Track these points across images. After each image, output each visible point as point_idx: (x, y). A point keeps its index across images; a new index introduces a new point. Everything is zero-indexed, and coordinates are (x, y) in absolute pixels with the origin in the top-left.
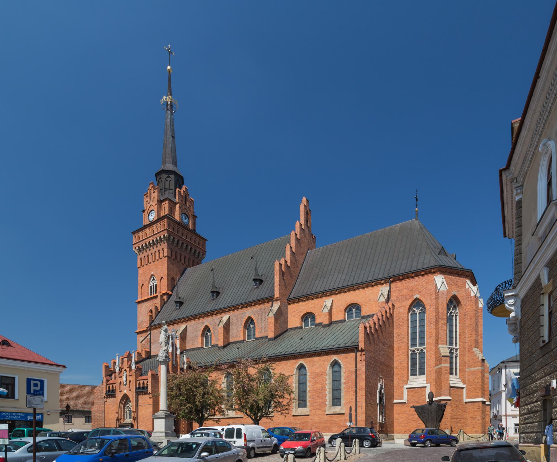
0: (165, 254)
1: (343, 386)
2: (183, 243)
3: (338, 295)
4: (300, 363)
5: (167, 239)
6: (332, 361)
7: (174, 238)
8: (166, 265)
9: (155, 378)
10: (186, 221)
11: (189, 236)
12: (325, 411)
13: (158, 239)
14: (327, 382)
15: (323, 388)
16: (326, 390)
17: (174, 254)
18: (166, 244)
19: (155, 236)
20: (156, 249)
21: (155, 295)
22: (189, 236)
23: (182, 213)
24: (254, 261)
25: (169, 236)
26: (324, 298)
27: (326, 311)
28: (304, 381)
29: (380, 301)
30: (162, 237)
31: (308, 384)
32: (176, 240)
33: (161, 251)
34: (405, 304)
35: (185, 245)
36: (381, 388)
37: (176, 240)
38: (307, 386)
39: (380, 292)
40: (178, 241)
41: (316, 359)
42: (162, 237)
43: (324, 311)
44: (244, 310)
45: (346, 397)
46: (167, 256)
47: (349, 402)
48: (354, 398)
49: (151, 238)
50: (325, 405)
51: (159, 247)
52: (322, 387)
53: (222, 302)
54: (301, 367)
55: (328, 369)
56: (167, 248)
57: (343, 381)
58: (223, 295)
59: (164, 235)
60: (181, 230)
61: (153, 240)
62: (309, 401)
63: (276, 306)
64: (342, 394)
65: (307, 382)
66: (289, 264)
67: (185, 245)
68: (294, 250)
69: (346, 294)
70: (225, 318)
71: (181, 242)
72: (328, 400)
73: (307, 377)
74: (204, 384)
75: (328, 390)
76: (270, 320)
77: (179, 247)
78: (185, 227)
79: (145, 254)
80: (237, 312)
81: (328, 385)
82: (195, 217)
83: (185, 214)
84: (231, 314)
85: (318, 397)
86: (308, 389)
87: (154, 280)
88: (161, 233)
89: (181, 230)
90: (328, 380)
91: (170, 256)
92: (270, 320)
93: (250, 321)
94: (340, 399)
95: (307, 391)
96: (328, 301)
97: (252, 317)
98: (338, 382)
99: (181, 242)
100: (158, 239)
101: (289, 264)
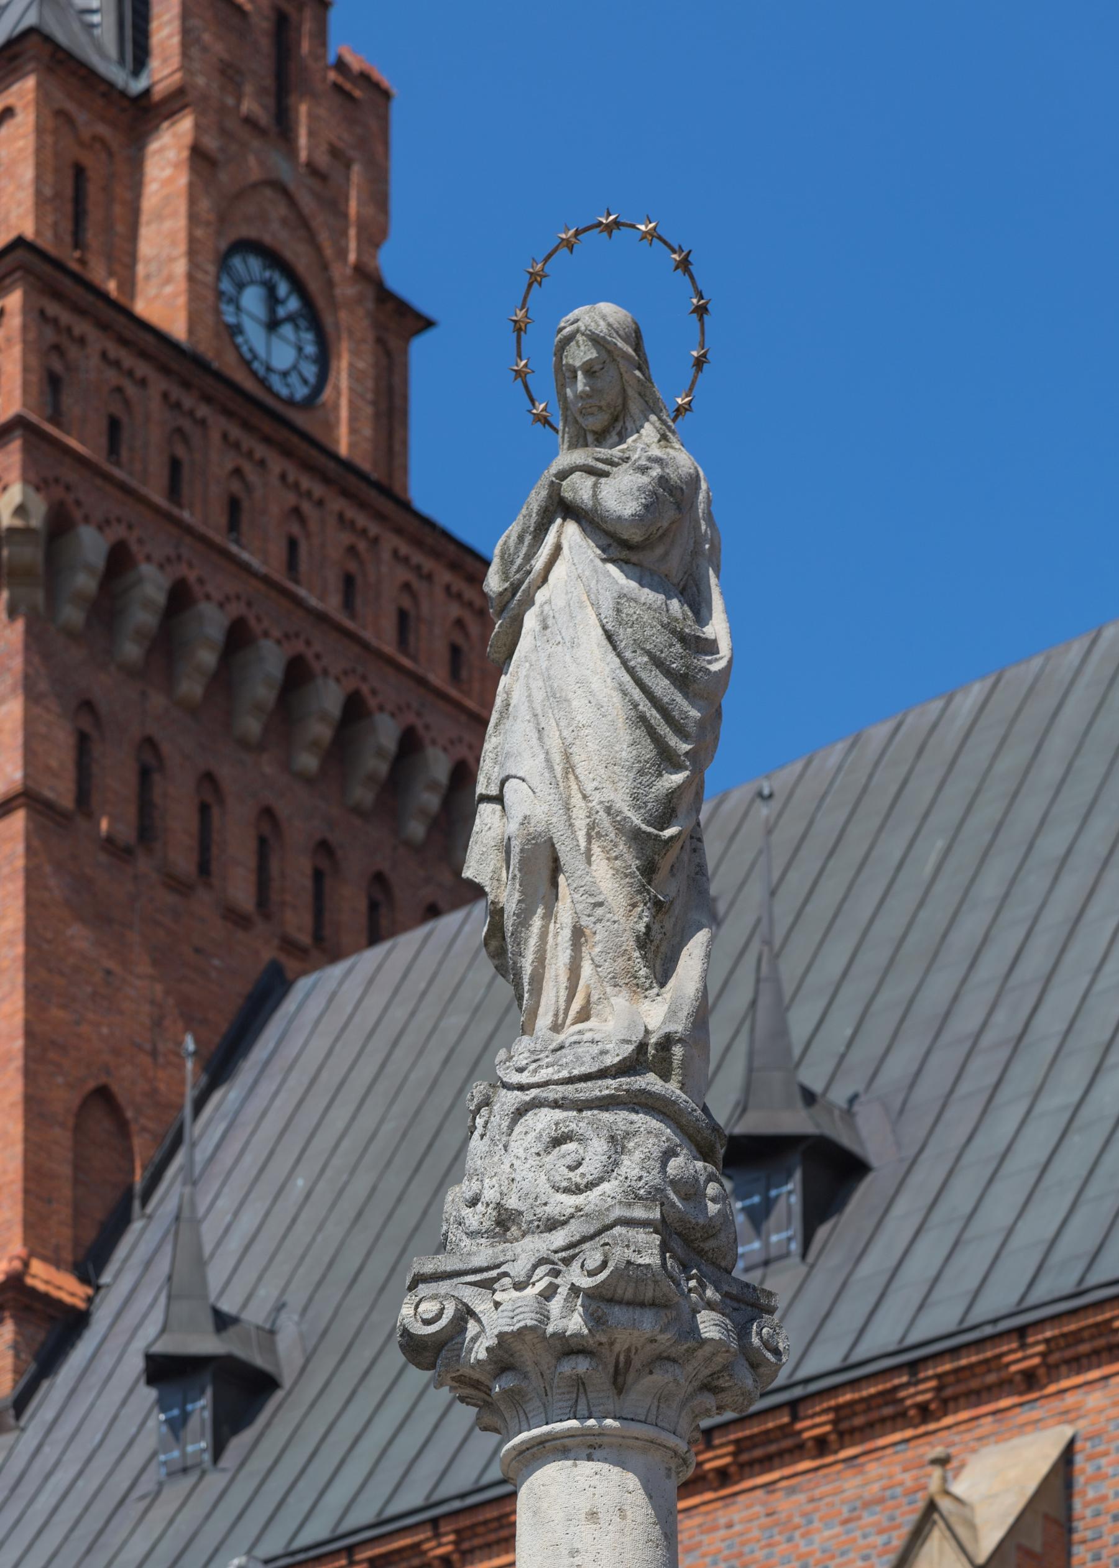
2: (238, 638)
7: (119, 560)
10: (282, 354)
11: (327, 542)
22: (327, 542)
23: (229, 247)
32: (152, 584)
35: (269, 661)
37: (152, 584)
40: (180, 598)
60: (220, 462)
67: (269, 661)
71: (211, 622)
78: (279, 425)
82: (399, 321)
83: (273, 258)
89: (220, 462)
91: (62, 792)
99: (211, 622)
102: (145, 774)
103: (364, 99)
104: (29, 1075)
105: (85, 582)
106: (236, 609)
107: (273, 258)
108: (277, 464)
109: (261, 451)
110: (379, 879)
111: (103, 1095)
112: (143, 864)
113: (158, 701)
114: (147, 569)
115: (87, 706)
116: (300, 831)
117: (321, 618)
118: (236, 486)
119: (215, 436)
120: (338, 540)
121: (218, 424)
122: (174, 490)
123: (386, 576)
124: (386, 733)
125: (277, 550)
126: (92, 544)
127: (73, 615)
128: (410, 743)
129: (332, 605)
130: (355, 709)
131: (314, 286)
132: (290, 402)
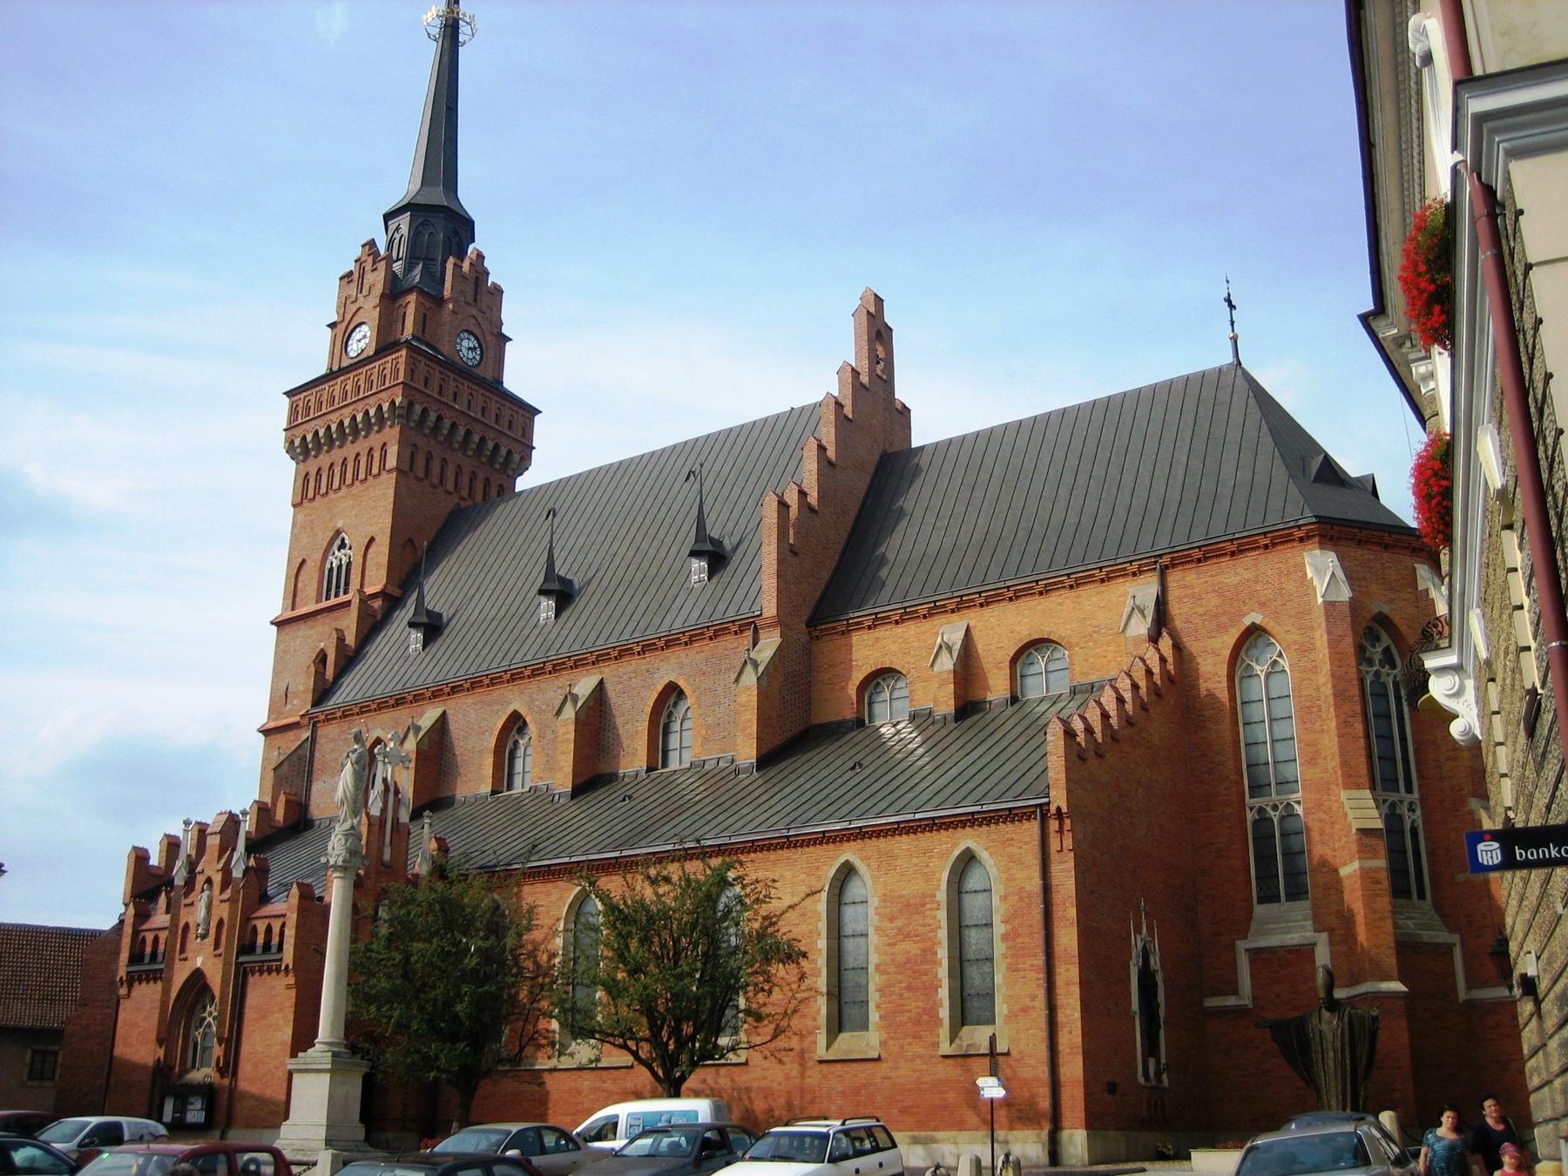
0: (392, 462)
1: (999, 949)
3: (987, 611)
4: (842, 860)
5: (402, 414)
6: (956, 853)
7: (425, 411)
8: (391, 499)
9: (313, 909)
12: (936, 1045)
13: (372, 412)
14: (943, 934)
15: (928, 954)
16: (936, 963)
18: (397, 429)
19: (360, 405)
20: (362, 446)
25: (411, 404)
26: (938, 620)
27: (947, 663)
28: (860, 928)
29: (1131, 632)
30: (385, 407)
31: (873, 938)
32: (433, 416)
33: (377, 455)
34: (1215, 643)
36: (1146, 953)
37: (433, 416)
38: (871, 949)
39: (1130, 602)
40: (440, 418)
41: (903, 843)
42: (385, 407)
43: (936, 668)
44: (651, 659)
45: (1013, 989)
47: (1025, 1010)
48: (1041, 994)
49: (347, 412)
50: (939, 1022)
51: (375, 440)
52: (924, 950)
53: (584, 627)
54: (847, 871)
55: (944, 886)
56: (400, 443)
57: (999, 928)
58: (584, 600)
59: (393, 402)
61: (354, 418)
62: (878, 1006)
64: (998, 979)
65: (871, 931)
66: (813, 498)
68: (831, 453)
69: (1011, 606)
70: (584, 686)
72: (946, 1003)
73: (871, 911)
74: (497, 925)
75: (945, 963)
76: (743, 699)
77: (441, 438)
79: (324, 460)
80: (630, 666)
81: (945, 943)
84: (608, 671)
85: (909, 988)
86: (874, 959)
88: (383, 395)
90: (944, 924)
91: (406, 467)
92: (743, 699)
93: (673, 692)
94: (990, 995)
95: (871, 968)
96: (951, 630)
97: (682, 683)
98: (985, 932)
100: (372, 412)
101: (813, 498)
105: (416, 417)
107: (471, 333)
110: (487, 479)
111: (410, 540)
115: (415, 445)
116: (467, 469)
117: (475, 419)
120: (481, 399)
122: (440, 393)
123: (493, 407)
124: (490, 445)
125: (466, 403)
126: (418, 409)
128: (496, 447)
129: (479, 416)
130: (483, 440)
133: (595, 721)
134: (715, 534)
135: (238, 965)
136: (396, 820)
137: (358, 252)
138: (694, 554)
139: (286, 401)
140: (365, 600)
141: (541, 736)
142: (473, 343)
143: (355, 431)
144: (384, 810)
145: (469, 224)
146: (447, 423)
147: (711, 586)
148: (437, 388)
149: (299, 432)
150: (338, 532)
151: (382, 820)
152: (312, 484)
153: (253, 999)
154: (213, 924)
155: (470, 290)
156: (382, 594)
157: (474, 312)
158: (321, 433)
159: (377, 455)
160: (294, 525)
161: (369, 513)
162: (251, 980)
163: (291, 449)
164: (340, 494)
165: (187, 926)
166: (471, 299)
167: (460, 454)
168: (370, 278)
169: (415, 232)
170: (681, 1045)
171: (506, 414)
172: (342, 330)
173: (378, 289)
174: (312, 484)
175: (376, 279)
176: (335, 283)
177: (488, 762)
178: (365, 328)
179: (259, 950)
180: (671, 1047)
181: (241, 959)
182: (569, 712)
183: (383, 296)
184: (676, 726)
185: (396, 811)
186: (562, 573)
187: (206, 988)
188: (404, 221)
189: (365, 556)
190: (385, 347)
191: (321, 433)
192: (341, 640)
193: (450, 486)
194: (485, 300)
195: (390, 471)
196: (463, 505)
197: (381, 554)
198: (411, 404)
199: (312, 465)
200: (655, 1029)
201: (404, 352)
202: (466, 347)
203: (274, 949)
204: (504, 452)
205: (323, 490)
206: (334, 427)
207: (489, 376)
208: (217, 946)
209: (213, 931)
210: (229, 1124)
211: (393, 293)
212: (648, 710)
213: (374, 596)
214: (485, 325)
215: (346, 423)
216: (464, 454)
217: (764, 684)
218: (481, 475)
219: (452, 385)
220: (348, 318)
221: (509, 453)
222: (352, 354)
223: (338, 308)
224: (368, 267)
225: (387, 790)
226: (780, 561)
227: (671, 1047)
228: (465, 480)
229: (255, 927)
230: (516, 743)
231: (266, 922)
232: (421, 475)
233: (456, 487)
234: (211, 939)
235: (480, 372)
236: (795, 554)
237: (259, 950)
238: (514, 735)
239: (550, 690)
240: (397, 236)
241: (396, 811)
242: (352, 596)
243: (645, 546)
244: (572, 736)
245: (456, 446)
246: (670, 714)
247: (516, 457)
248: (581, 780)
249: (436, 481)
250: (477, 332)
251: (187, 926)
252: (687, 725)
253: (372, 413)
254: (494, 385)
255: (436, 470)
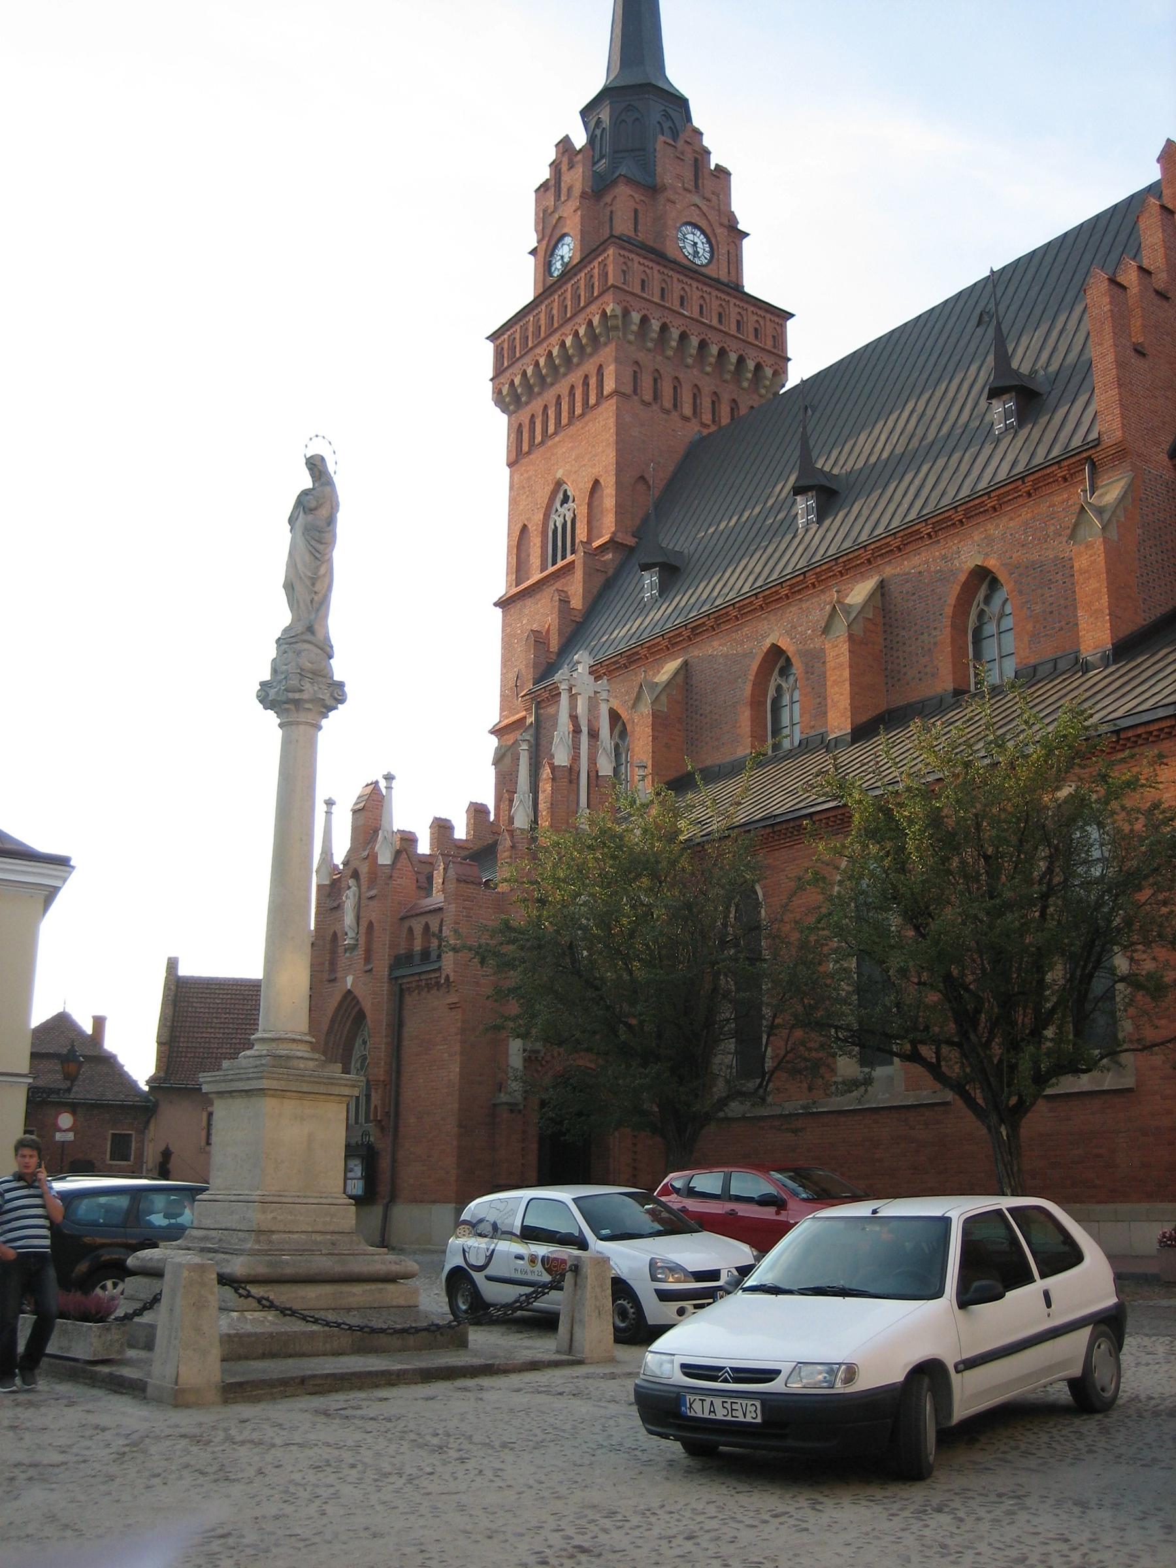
0: (609, 386)
2: (683, 337)
7: (644, 320)
8: (613, 430)
17: (646, 381)
21: (570, 558)
24: (991, 332)
25: (626, 313)
30: (596, 320)
33: (593, 381)
37: (655, 325)
42: (596, 320)
46: (616, 392)
49: (554, 339)
51: (590, 367)
56: (617, 360)
59: (604, 313)
63: (1112, 491)
77: (670, 353)
79: (536, 406)
87: (566, 500)
89: (677, 287)
91: (628, 389)
97: (992, 563)
102: (655, 380)
103: (722, 174)
104: (617, 475)
106: (682, 329)
108: (695, 284)
109: (689, 281)
111: (642, 478)
112: (655, 407)
113: (659, 358)
114: (653, 321)
115: (637, 363)
118: (682, 293)
119: (675, 280)
121: (676, 276)
122: (662, 297)
127: (631, 337)
131: (708, 231)
132: (702, 266)
133: (881, 636)
134: (1025, 369)
135: (393, 979)
136: (594, 777)
137: (552, 155)
138: (995, 393)
139: (490, 346)
140: (592, 555)
141: (809, 671)
142: (699, 239)
143: (567, 359)
144: (576, 758)
145: (682, 103)
146: (675, 333)
147: (1024, 432)
148: (657, 291)
149: (502, 379)
150: (559, 484)
151: (572, 773)
152: (526, 436)
153: (411, 1027)
154: (363, 929)
155: (689, 175)
156: (612, 544)
157: (697, 200)
158: (530, 371)
159: (593, 381)
160: (511, 488)
161: (590, 456)
162: (409, 1000)
163: (500, 400)
164: (557, 439)
165: (335, 934)
166: (690, 185)
167: (695, 372)
168: (567, 178)
169: (616, 122)
170: (1013, 1046)
171: (751, 320)
172: (544, 253)
173: (577, 192)
174: (526, 436)
175: (576, 178)
176: (532, 197)
177: (745, 716)
178: (568, 240)
179: (417, 959)
180: (997, 1050)
181: (396, 973)
182: (841, 627)
183: (583, 195)
184: (990, 628)
185: (592, 760)
186: (827, 469)
187: (361, 1016)
188: (605, 115)
189: (590, 505)
190: (589, 254)
191: (530, 371)
192: (564, 602)
193: (687, 410)
194: (708, 184)
195: (610, 396)
196: (705, 432)
197: (609, 499)
198: (626, 313)
199: (524, 416)
200: (966, 1019)
201: (611, 251)
202: (693, 244)
203: (434, 956)
204: (751, 365)
205: (538, 439)
206: (542, 361)
207: (724, 277)
208: (368, 959)
209: (362, 940)
210: (393, 1198)
211: (598, 190)
212: (949, 611)
213: (603, 548)
214: (712, 215)
215: (555, 352)
216: (702, 371)
217: (1113, 535)
218: (725, 398)
219: (676, 289)
220: (548, 232)
221: (758, 367)
222: (556, 274)
223: (537, 224)
224: (564, 167)
225: (577, 731)
226: (1120, 364)
227: (997, 1050)
228: (706, 403)
229: (411, 930)
230: (779, 688)
231: (423, 920)
232: (648, 397)
233: (695, 412)
234: (360, 952)
235: (711, 271)
236: (1140, 352)
237: (417, 959)
238: (775, 680)
239: (815, 609)
240: (598, 132)
241: (592, 760)
242: (577, 558)
243: (930, 412)
244: (845, 658)
245: (690, 361)
246: (981, 614)
247: (769, 372)
248: (864, 718)
249: (668, 404)
250: (703, 223)
251: (335, 934)
252: (1008, 623)
253: (582, 332)
254: (735, 288)
255: (667, 389)
